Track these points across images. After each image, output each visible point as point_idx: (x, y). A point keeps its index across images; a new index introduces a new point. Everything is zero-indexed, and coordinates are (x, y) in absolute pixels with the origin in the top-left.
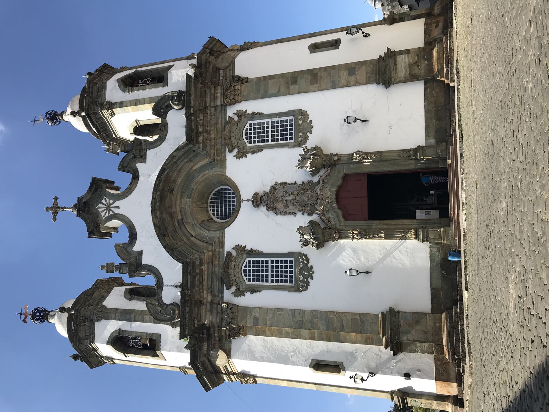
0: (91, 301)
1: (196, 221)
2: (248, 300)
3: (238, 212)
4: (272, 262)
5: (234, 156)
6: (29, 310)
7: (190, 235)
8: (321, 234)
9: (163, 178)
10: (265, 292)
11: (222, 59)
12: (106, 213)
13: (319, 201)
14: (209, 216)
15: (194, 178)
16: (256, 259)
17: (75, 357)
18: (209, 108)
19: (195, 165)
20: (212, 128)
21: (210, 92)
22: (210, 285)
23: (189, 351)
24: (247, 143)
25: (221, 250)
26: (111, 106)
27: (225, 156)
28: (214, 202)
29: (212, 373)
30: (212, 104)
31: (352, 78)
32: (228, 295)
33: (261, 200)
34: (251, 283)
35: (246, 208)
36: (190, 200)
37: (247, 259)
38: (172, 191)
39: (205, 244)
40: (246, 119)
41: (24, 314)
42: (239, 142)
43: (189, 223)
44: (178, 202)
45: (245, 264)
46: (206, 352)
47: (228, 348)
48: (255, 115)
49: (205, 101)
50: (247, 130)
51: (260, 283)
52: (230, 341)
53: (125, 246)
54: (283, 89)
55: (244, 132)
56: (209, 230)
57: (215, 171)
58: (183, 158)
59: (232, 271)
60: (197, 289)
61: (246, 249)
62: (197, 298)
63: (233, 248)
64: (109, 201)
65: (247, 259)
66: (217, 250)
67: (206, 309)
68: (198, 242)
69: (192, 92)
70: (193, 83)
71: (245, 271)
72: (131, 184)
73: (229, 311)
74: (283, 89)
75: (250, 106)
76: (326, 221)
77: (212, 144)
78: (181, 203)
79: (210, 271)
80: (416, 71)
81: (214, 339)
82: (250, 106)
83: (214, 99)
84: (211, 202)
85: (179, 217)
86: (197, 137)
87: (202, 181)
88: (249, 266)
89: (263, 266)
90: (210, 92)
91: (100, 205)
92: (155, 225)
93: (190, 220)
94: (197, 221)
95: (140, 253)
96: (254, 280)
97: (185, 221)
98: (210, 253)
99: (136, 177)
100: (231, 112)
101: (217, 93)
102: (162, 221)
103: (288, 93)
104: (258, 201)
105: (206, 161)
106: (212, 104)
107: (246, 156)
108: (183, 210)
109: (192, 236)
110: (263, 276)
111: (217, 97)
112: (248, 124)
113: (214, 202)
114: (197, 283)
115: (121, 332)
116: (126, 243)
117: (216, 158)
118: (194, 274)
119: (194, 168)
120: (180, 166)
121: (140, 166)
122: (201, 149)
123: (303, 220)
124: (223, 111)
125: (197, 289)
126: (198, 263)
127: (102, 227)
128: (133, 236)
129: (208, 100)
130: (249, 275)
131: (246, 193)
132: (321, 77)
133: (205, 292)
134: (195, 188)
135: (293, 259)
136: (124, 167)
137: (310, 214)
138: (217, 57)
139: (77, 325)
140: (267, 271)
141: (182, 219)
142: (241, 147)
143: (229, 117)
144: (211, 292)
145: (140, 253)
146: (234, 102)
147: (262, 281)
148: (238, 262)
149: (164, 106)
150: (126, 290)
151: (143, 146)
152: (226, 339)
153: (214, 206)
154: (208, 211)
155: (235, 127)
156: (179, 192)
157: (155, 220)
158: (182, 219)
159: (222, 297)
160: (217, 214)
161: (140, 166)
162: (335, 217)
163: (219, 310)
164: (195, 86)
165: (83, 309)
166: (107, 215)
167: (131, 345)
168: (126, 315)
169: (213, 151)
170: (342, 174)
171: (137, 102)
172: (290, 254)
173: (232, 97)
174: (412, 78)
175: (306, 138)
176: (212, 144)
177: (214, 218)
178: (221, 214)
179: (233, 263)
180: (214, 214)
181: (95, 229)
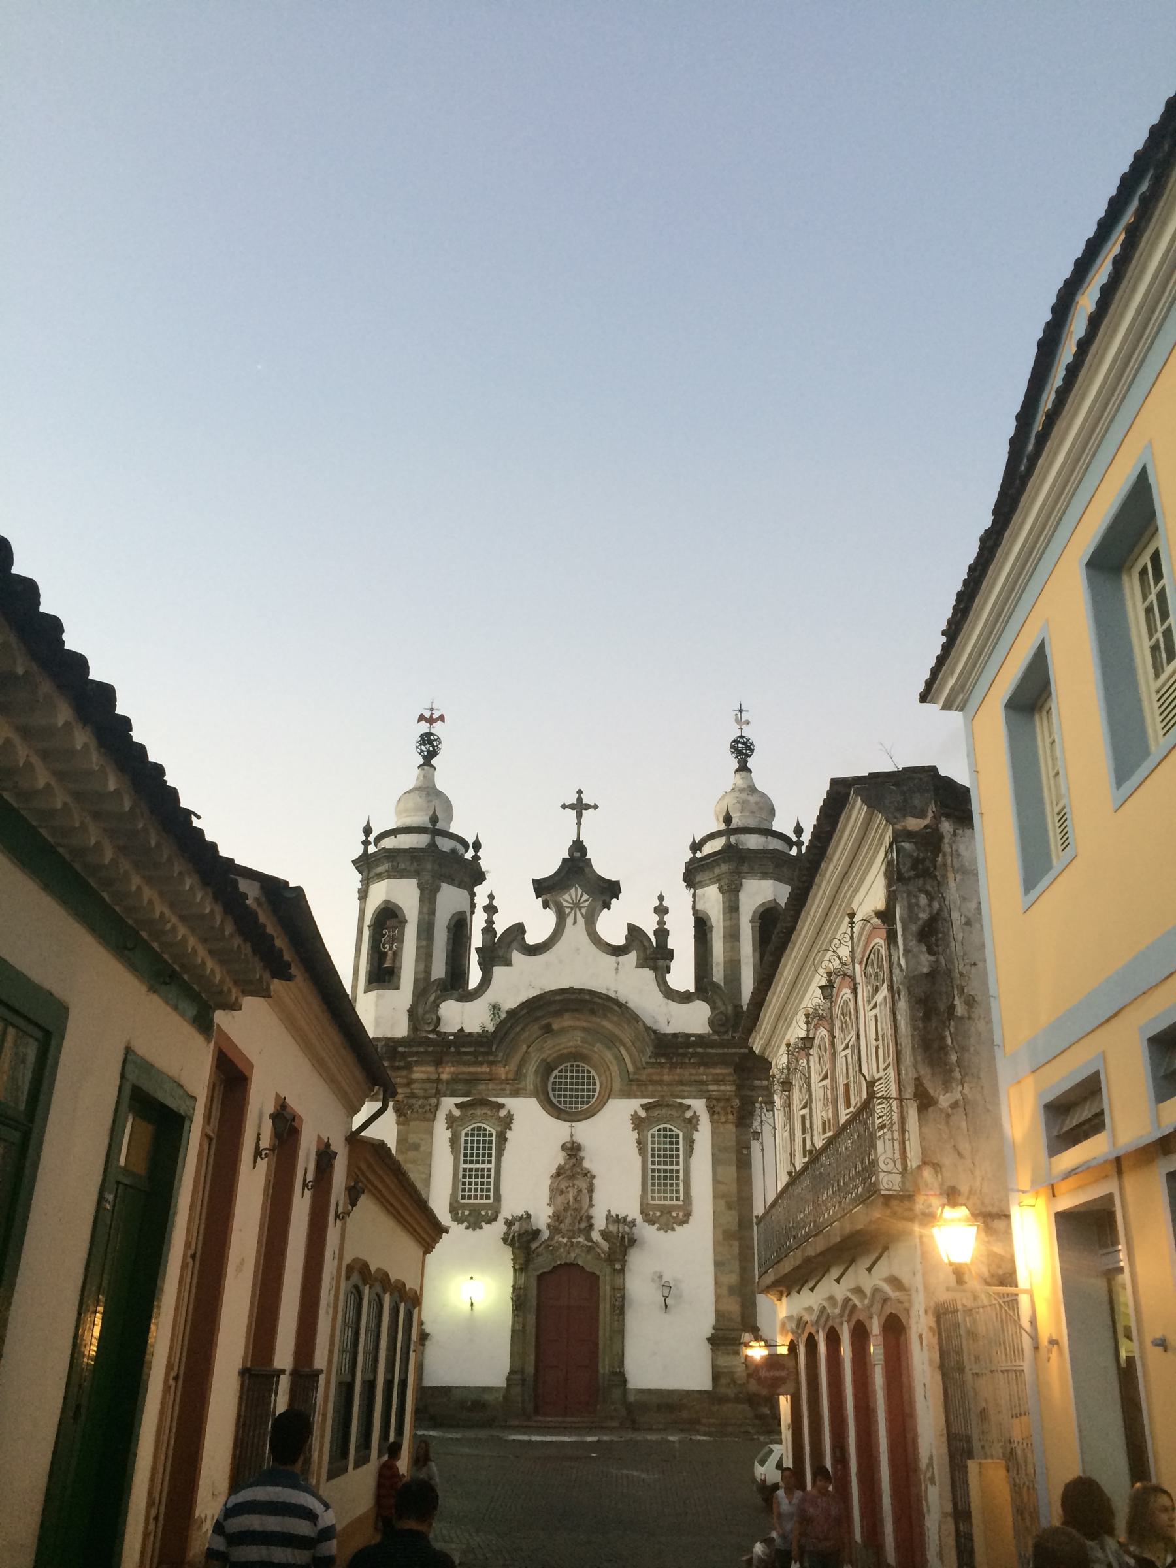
2: (441, 1134)
4: (489, 1170)
6: (438, 729)
8: (522, 1241)
10: (451, 1158)
13: (565, 1240)
15: (609, 1048)
16: (494, 1145)
17: (367, 831)
19: (627, 1049)
20: (676, 1078)
21: (730, 1074)
24: (651, 1131)
26: (731, 893)
28: (577, 1071)
30: (710, 1078)
31: (725, 1291)
34: (463, 1139)
35: (560, 1131)
38: (593, 1012)
44: (578, 1023)
45: (488, 1128)
48: (690, 1143)
50: (671, 1130)
51: (462, 1151)
53: (519, 938)
54: (722, 1188)
59: (479, 1111)
62: (445, 1059)
69: (726, 1050)
70: (738, 1050)
71: (479, 1128)
73: (428, 1108)
74: (722, 1188)
75: (704, 1136)
76: (540, 1250)
78: (575, 1028)
80: (723, 1381)
82: (704, 1136)
83: (718, 1081)
85: (555, 1027)
86: (663, 1055)
88: (485, 1135)
89: (483, 1155)
90: (730, 1074)
91: (580, 891)
93: (550, 1043)
95: (508, 963)
96: (466, 1142)
98: (503, 1077)
100: (698, 1105)
102: (550, 1003)
103: (716, 1196)
104: (573, 1150)
105: (631, 1069)
107: (634, 1129)
109: (528, 1047)
110: (472, 1155)
113: (577, 1071)
114: (465, 1058)
121: (633, 956)
123: (542, 1217)
126: (491, 1058)
128: (533, 950)
129: (718, 1071)
130: (473, 1135)
131: (586, 1132)
132: (731, 1246)
133: (453, 1069)
135: (491, 1201)
136: (634, 931)
137: (549, 1226)
140: (477, 1162)
145: (508, 963)
146: (711, 1110)
147: (465, 1155)
150: (463, 913)
151: (661, 963)
153: (572, 1071)
156: (589, 1025)
161: (633, 956)
162: (544, 1263)
164: (735, 1053)
166: (565, 904)
168: (426, 931)
169: (644, 1077)
170: (598, 1273)
171: (732, 936)
172: (498, 1198)
173: (717, 1109)
174: (716, 1377)
175: (651, 1222)
177: (556, 1073)
178: (560, 1083)
181: (542, 888)
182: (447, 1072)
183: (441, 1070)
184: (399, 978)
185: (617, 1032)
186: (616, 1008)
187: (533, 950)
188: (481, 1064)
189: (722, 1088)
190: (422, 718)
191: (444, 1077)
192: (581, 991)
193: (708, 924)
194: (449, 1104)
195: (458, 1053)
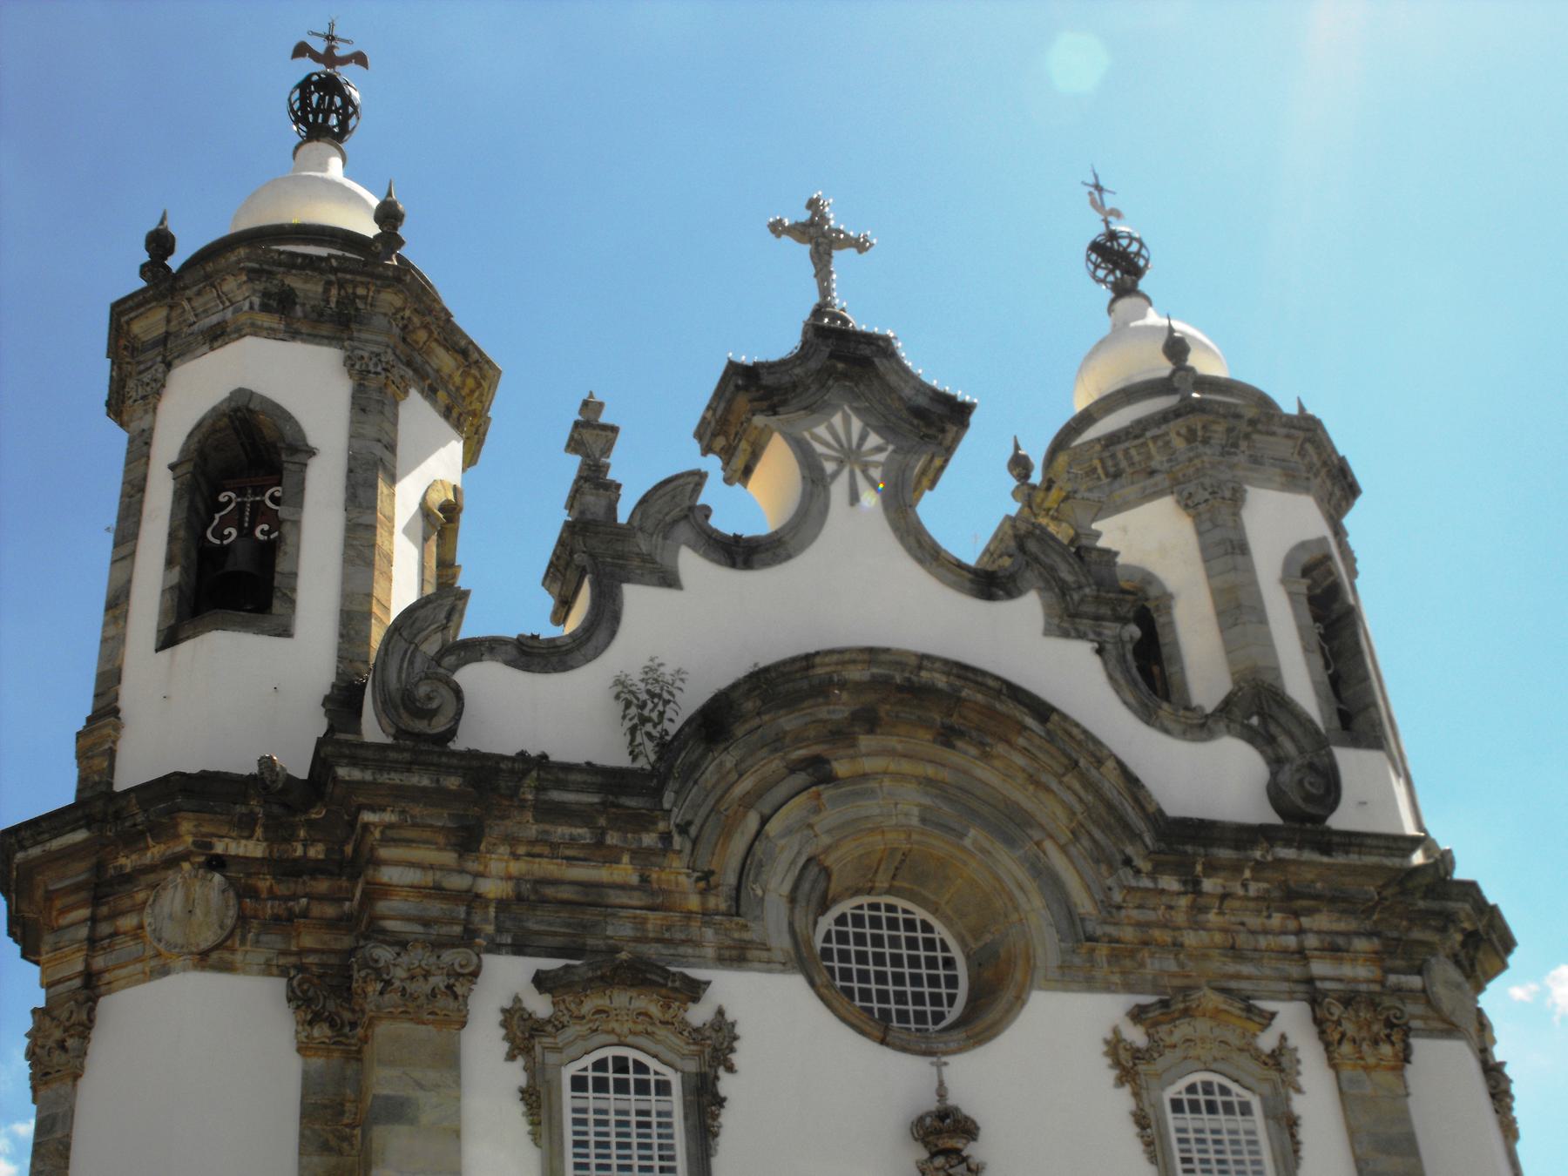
0: (422, 335)
1: (826, 840)
3: (883, 1042)
5: (1116, 1031)
7: (767, 811)
9: (1007, 707)
11: (1458, 986)
12: (827, 445)
14: (835, 901)
15: (1010, 842)
18: (1292, 924)
19: (1063, 849)
21: (1358, 934)
22: (549, 891)
23: (255, 770)
25: (710, 952)
27: (1108, 988)
28: (893, 924)
29: (100, 867)
32: (507, 978)
33: (947, 1152)
36: (915, 821)
37: (675, 1080)
38: (948, 736)
39: (732, 879)
40: (1266, 1089)
41: (330, 49)
42: (1179, 1053)
43: (817, 810)
46: (219, 848)
47: (238, 957)
48: (1287, 1125)
49: (1318, 911)
52: (267, 970)
55: (1216, 1079)
56: (792, 900)
57: (1046, 943)
58: (1089, 798)
60: (533, 830)
61: (721, 1072)
62: (495, 830)
63: (720, 1012)
64: (876, 464)
65: (675, 1080)
66: (709, 933)
67: (442, 868)
68: (739, 844)
71: (621, 1065)
72: (960, 565)
73: (438, 980)
77: (1157, 933)
78: (900, 777)
79: (616, 898)
81: (281, 890)
83: (1334, 949)
84: (891, 908)
85: (841, 768)
87: (998, 879)
91: (857, 425)
92: (808, 660)
93: (831, 817)
94: (828, 849)
95: (669, 579)
97: (827, 792)
98: (694, 902)
99: (988, 583)
100: (1291, 1021)
101: (1354, 960)
102: (822, 689)
105: (1084, 904)
106: (1311, 941)
108: (873, 784)
109: (764, 821)
111: (1340, 960)
112: (1247, 1096)
114: (562, 831)
115: (298, 458)
116: (707, 517)
117: (1103, 950)
118: (602, 822)
119: (1048, 845)
120: (1054, 785)
121: (1029, 608)
122: (1133, 883)
124: (1285, 986)
125: (533, 830)
127: (772, 421)
128: (740, 553)
134: (967, 842)
138: (1458, 963)
139: (335, 271)
141: (829, 779)
142: (1161, 1063)
143: (1273, 1015)
144: (519, 898)
145: (669, 579)
148: (662, 1032)
149: (1273, 729)
152: (283, 953)
154: (857, 892)
155: (1235, 1040)
156: (945, 775)
157: (835, 657)
158: (829, 779)
159: (495, 948)
160: (843, 938)
161: (1029, 608)
163: (444, 930)
165: (398, 301)
166: (819, 448)
167: (223, 498)
169: (1129, 934)
173: (1349, 1028)
176: (1157, 933)
179: (654, 1010)
180: (841, 920)
182: (497, 872)
183: (472, 866)
184: (292, 602)
185: (1022, 796)
186: (1030, 721)
187: (740, 553)
188: (612, 858)
189: (1347, 970)
190: (301, 50)
191: (492, 888)
192: (924, 660)
193: (1153, 592)
194: (507, 978)
195: (551, 812)
